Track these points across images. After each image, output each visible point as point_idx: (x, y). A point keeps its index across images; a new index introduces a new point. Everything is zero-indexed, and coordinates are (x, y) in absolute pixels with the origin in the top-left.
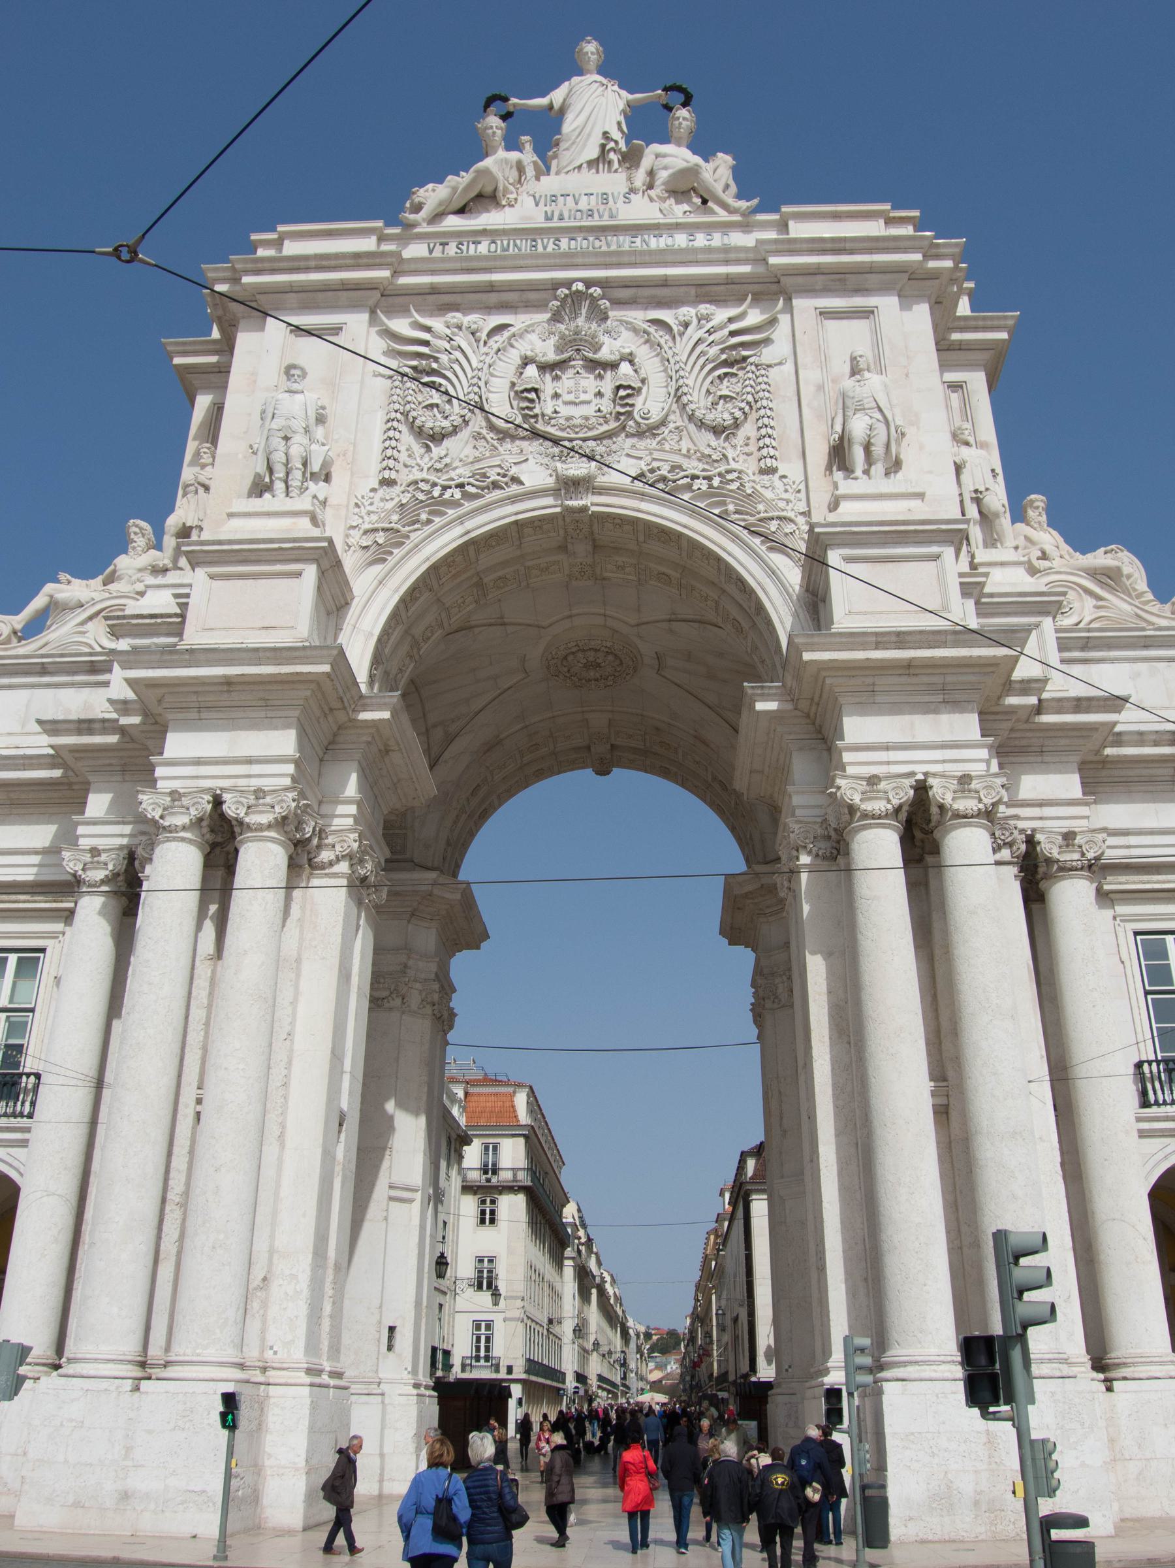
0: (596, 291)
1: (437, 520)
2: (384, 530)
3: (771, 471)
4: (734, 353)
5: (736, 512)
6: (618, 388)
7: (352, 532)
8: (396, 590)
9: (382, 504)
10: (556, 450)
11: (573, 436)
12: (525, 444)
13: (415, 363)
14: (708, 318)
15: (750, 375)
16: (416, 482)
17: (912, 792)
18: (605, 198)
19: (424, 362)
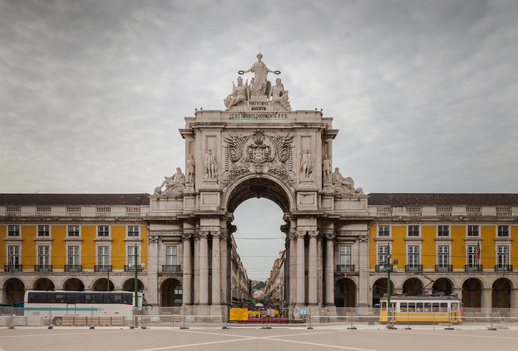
0: (262, 131)
1: (236, 178)
2: (227, 180)
3: (291, 170)
4: (286, 145)
5: (285, 179)
6: (266, 154)
7: (222, 180)
8: (230, 192)
9: (226, 175)
10: (255, 165)
11: (258, 162)
12: (249, 163)
13: (230, 145)
14: (282, 137)
15: (288, 150)
16: (232, 171)
17: (306, 233)
18: (263, 103)
19: (231, 145)
